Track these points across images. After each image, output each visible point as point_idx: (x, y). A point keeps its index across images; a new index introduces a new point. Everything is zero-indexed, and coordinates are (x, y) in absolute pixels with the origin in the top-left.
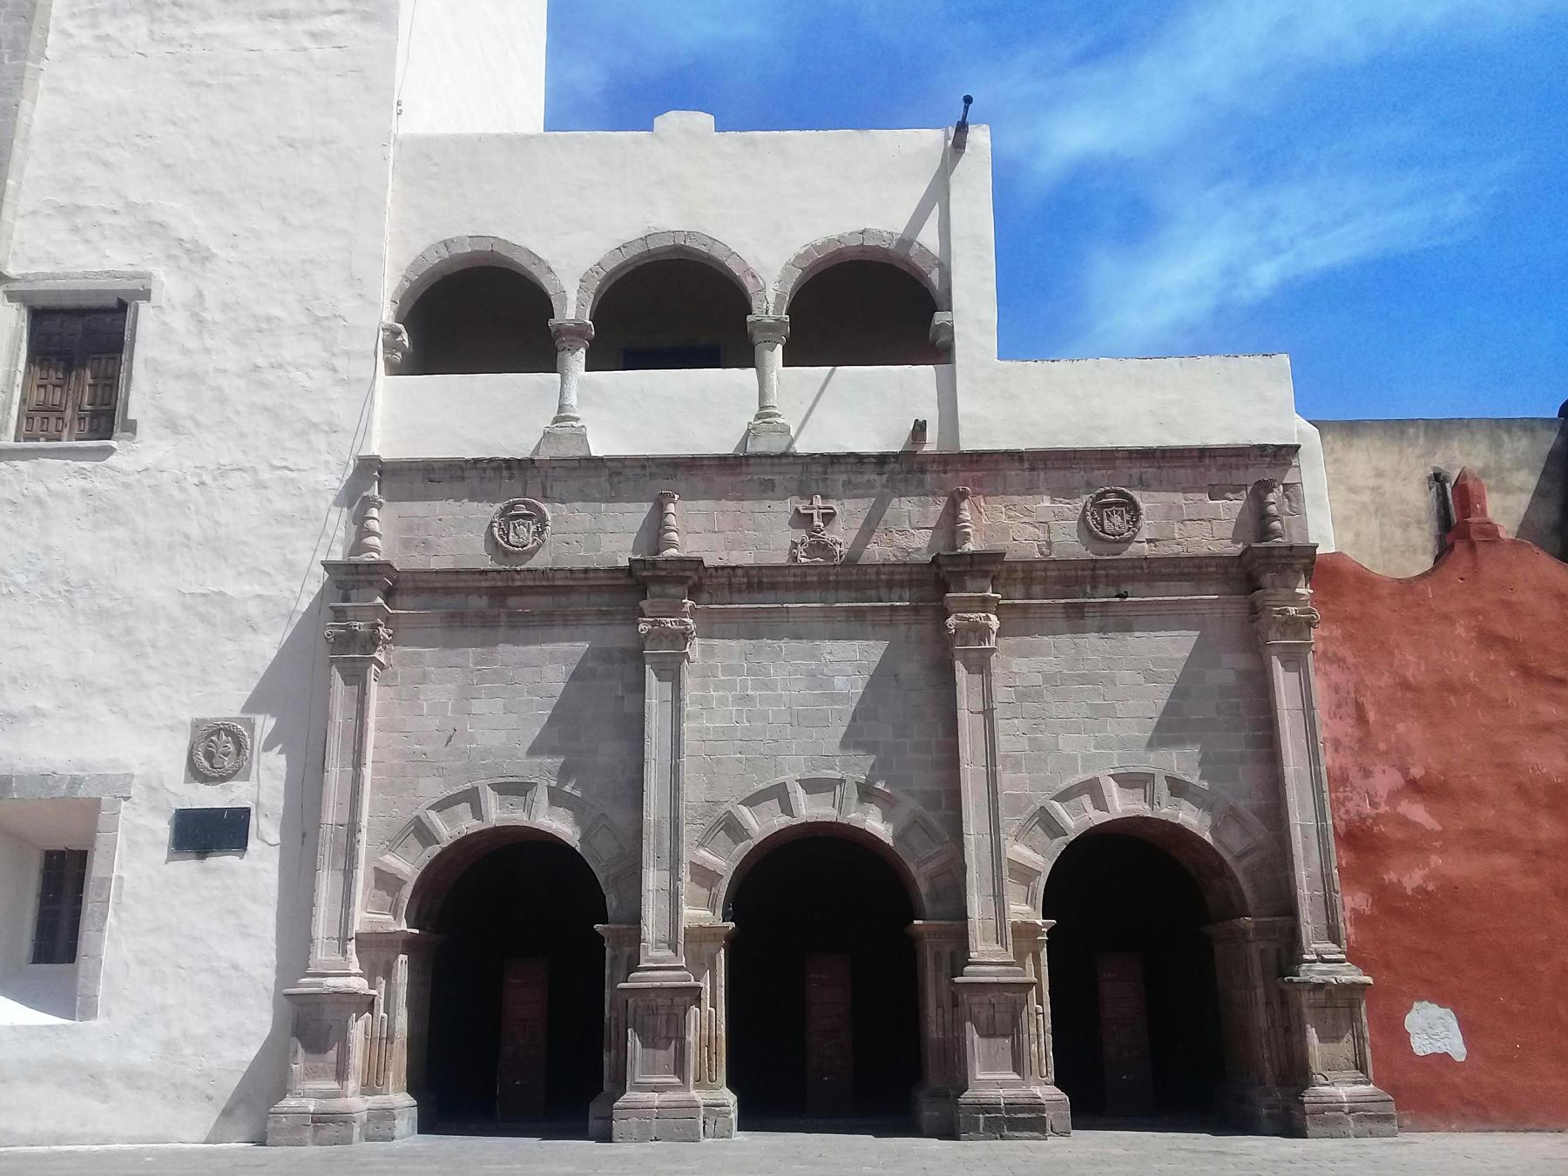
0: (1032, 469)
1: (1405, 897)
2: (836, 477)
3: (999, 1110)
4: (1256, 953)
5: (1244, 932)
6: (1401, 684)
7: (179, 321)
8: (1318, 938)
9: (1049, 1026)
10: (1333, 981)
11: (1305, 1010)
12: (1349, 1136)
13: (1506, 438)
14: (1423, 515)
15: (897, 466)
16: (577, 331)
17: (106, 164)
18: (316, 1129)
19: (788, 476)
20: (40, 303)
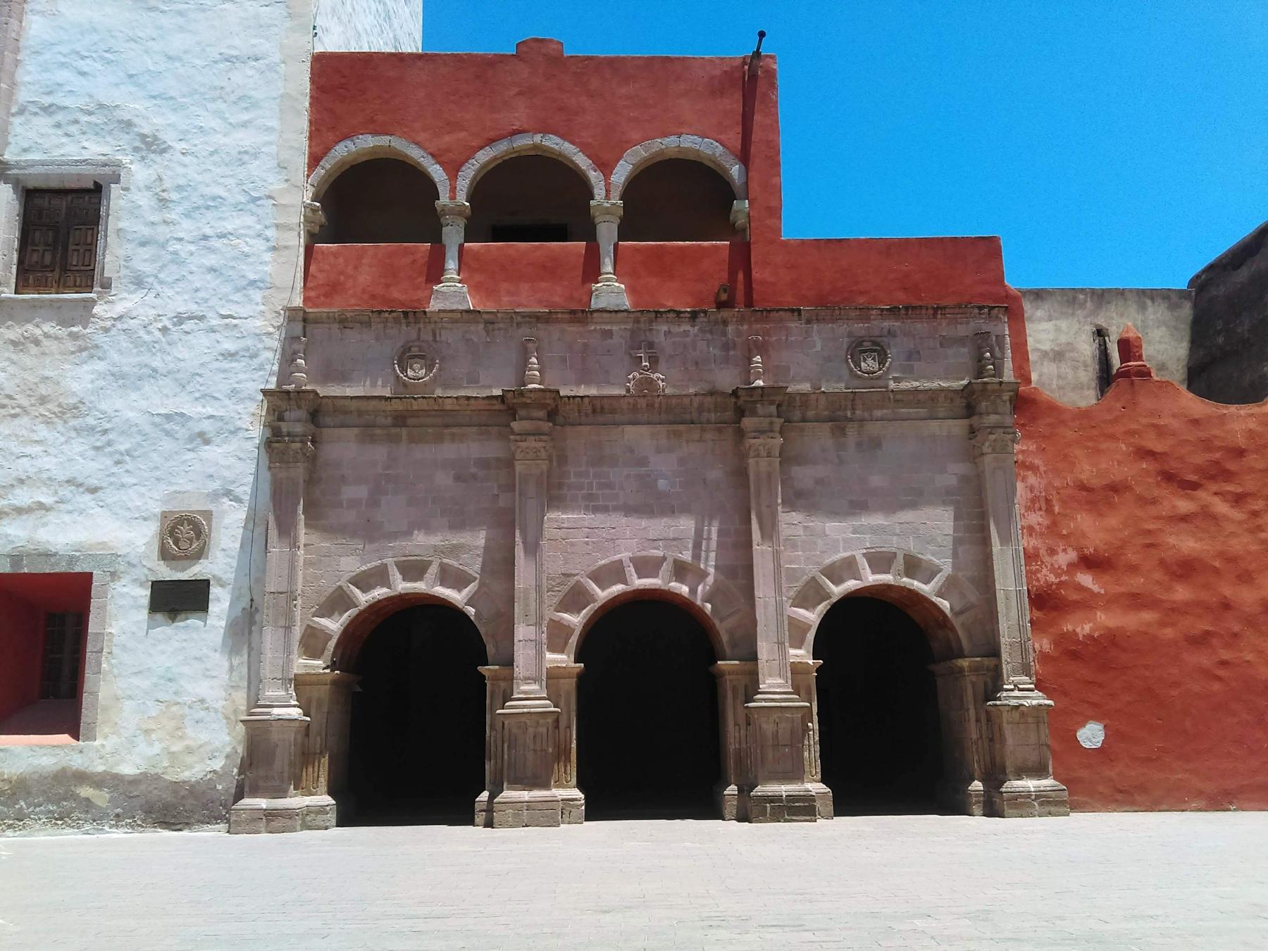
0: (809, 322)
1: (1078, 642)
2: (659, 328)
3: (781, 801)
4: (970, 686)
5: (961, 670)
6: (1078, 486)
7: (144, 200)
8: (1015, 672)
9: (817, 738)
10: (1025, 703)
11: (1005, 725)
12: (1034, 816)
13: (1149, 302)
14: (1089, 361)
15: (705, 319)
16: (458, 212)
17: (83, 74)
18: (268, 821)
19: (623, 327)
20: (31, 184)
